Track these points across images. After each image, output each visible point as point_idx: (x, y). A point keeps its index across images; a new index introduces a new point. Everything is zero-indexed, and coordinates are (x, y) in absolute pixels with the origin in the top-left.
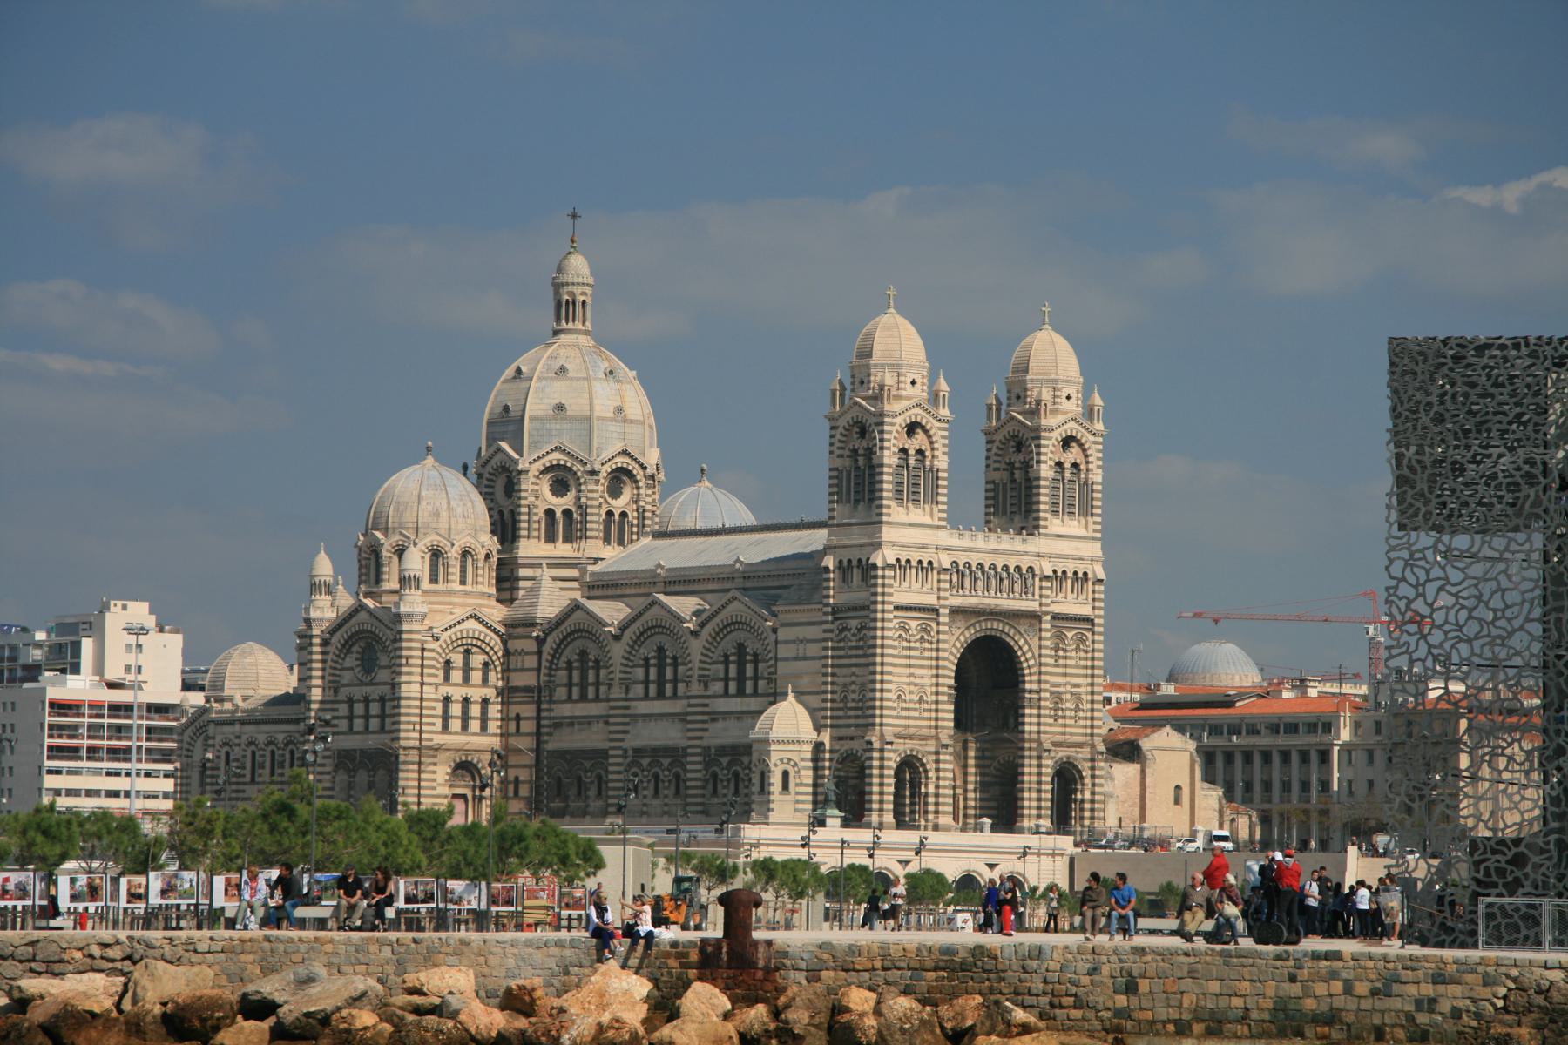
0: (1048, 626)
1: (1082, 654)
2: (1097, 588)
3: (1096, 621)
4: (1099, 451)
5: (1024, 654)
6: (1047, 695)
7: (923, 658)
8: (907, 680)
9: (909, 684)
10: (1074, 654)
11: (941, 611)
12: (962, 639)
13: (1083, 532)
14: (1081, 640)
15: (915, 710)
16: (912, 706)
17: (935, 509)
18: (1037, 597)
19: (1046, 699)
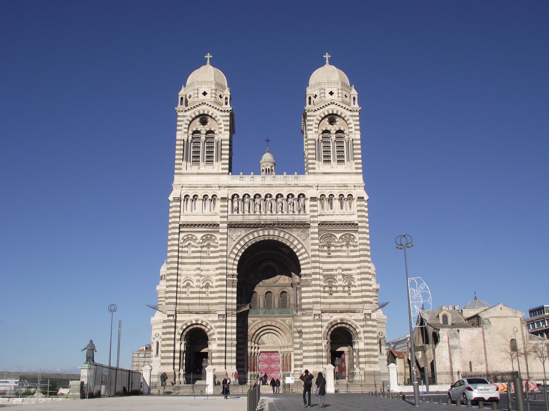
0: (317, 230)
1: (352, 248)
2: (359, 203)
3: (359, 224)
4: (356, 121)
5: (299, 250)
6: (317, 276)
7: (210, 258)
8: (193, 272)
9: (198, 275)
10: (345, 248)
11: (221, 225)
12: (242, 243)
13: (349, 170)
14: (348, 240)
15: (200, 292)
16: (198, 290)
17: (220, 163)
18: (308, 212)
19: (316, 279)
